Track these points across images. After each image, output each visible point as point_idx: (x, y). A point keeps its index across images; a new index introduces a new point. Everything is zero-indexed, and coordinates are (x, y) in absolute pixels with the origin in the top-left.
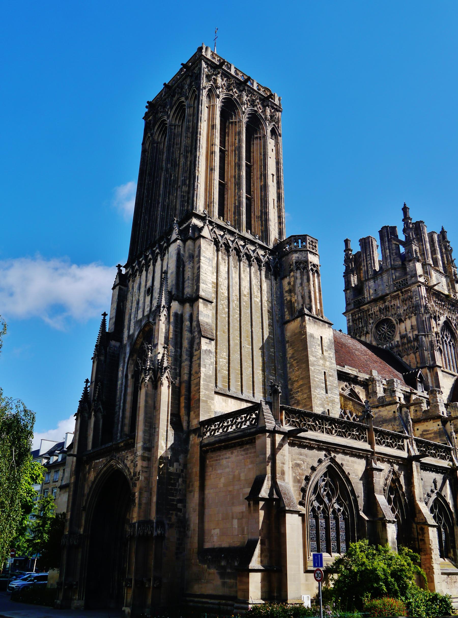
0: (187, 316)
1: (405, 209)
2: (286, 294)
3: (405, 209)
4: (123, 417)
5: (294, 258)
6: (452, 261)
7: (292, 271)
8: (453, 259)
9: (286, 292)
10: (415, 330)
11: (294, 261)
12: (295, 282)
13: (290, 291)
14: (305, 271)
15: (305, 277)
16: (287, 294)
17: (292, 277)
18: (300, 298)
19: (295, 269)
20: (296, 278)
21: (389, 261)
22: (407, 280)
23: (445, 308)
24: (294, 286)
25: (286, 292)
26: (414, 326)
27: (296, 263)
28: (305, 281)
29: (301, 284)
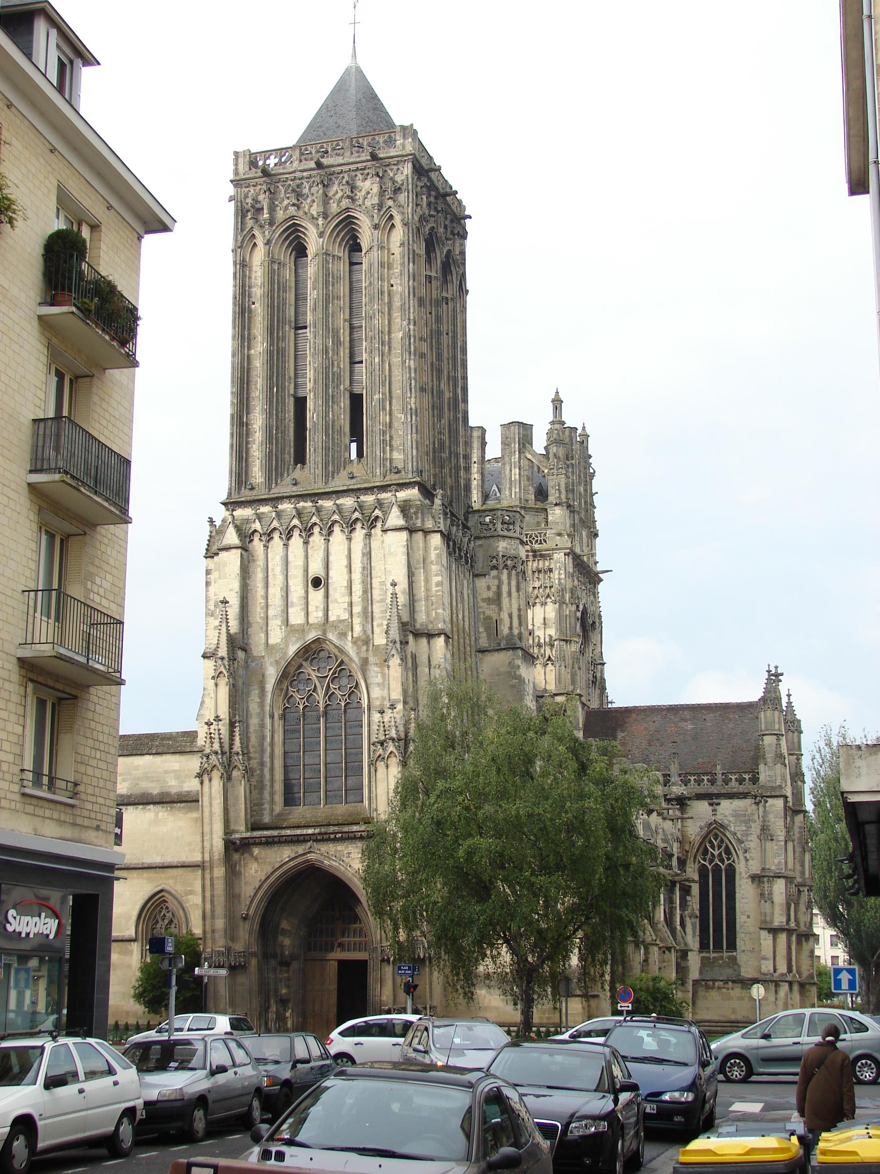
0: (423, 659)
1: (557, 403)
2: (482, 604)
3: (557, 403)
4: (272, 780)
5: (500, 549)
6: (592, 495)
7: (495, 567)
8: (594, 491)
9: (484, 600)
10: (551, 627)
11: (501, 554)
12: (499, 587)
13: (489, 601)
14: (514, 572)
15: (514, 583)
16: (485, 604)
17: (494, 578)
18: (505, 616)
19: (501, 568)
20: (500, 580)
21: (518, 490)
22: (545, 535)
23: (583, 588)
24: (499, 594)
25: (484, 600)
26: (549, 619)
27: (503, 556)
28: (514, 589)
29: (509, 594)
